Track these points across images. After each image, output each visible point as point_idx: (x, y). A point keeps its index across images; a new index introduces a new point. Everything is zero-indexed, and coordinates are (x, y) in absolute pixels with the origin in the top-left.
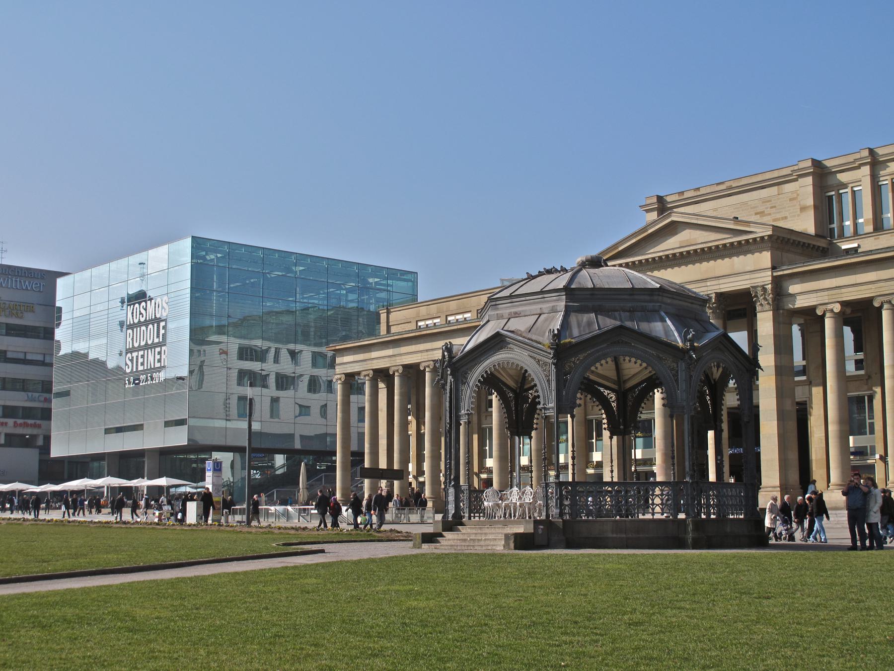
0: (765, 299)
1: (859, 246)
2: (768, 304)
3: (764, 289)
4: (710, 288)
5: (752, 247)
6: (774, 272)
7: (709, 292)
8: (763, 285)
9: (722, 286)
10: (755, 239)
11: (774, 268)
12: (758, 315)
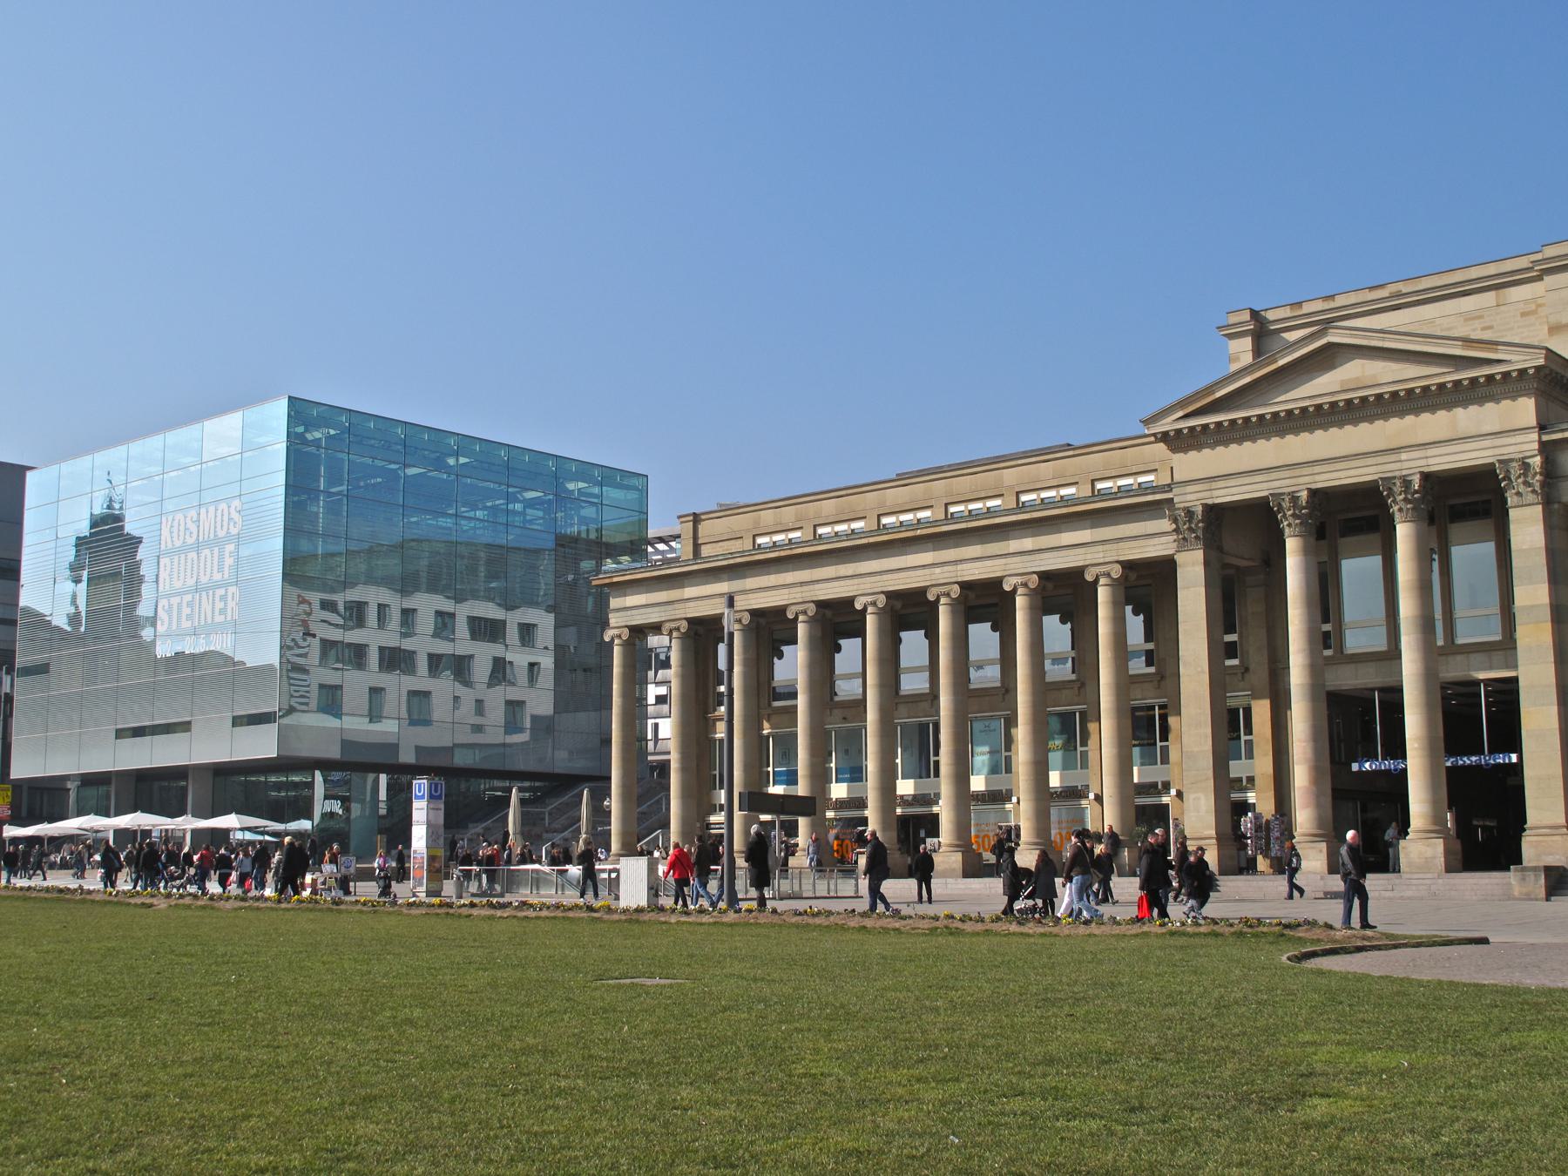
0: (1526, 483)
2: (1534, 491)
6: (1544, 434)
7: (1404, 473)
8: (1523, 458)
9: (1431, 461)
10: (1506, 375)
12: (1511, 512)
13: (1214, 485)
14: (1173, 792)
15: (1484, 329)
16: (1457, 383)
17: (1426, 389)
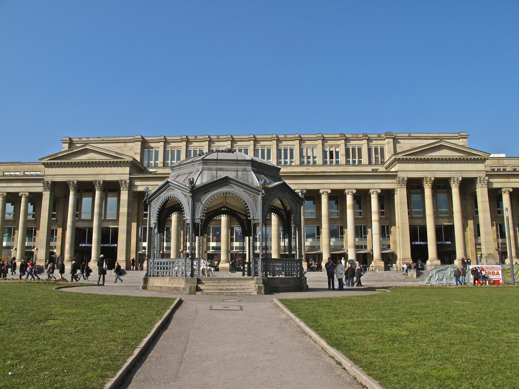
0: (125, 186)
1: (156, 171)
2: (127, 188)
3: (126, 182)
4: (100, 178)
5: (122, 165)
9: (105, 178)
10: (124, 162)
11: (130, 174)
13: (55, 177)
14: (36, 249)
15: (121, 151)
16: (113, 162)
17: (106, 162)
